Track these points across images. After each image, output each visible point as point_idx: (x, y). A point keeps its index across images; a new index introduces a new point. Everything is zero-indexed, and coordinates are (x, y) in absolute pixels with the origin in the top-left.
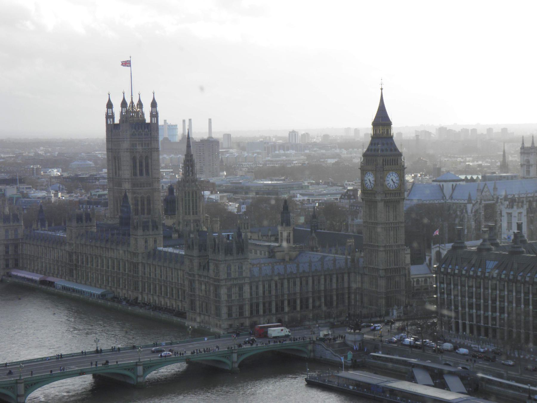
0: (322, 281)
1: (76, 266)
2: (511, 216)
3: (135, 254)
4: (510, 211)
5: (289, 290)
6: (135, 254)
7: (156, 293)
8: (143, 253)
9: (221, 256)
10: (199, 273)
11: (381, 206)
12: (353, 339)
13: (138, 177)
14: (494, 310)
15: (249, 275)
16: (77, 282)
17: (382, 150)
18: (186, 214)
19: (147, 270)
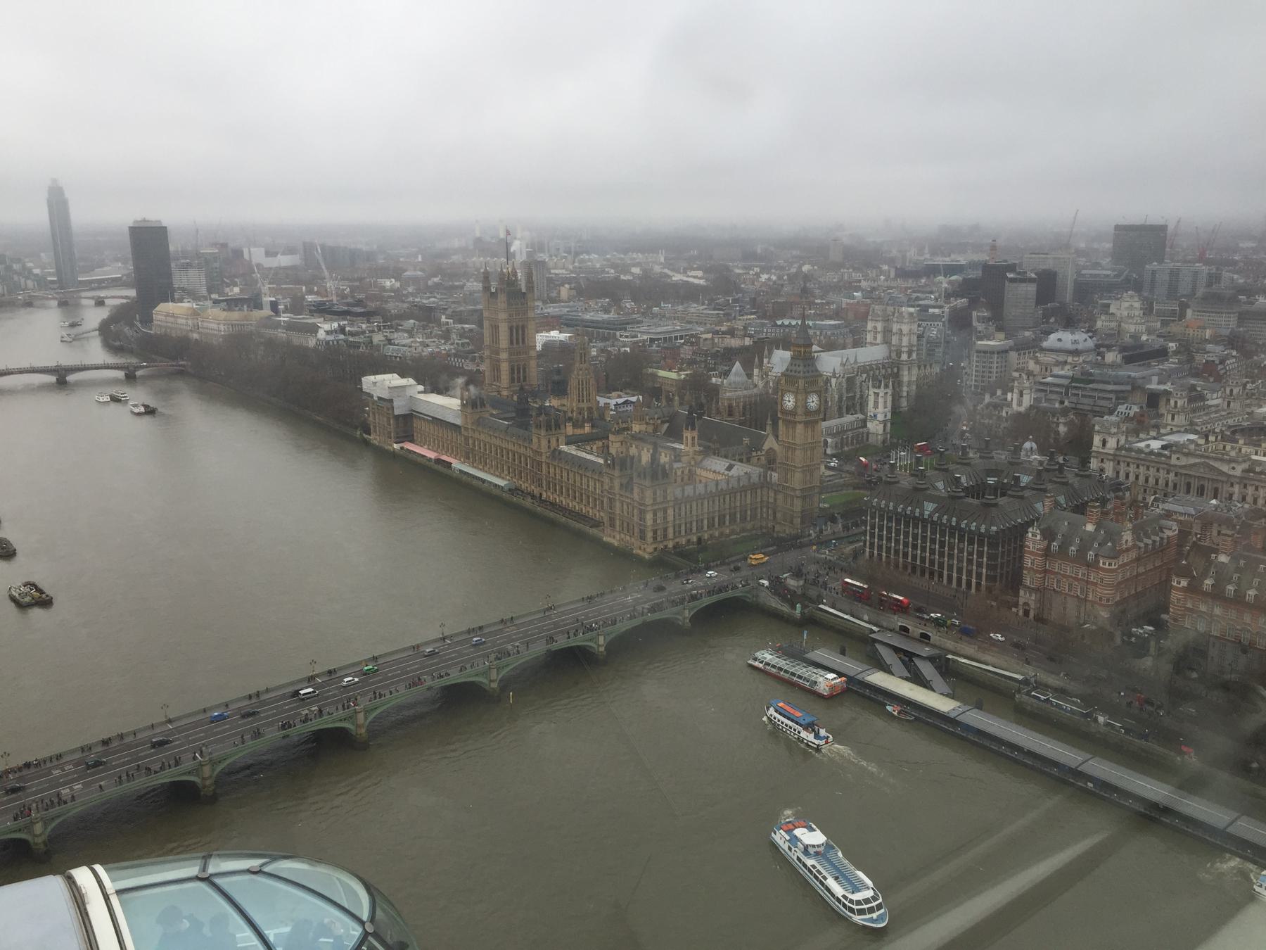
0: (738, 498)
1: (473, 450)
2: (878, 396)
3: (538, 452)
4: (876, 391)
5: (708, 509)
6: (540, 454)
7: (562, 493)
8: (546, 453)
9: (647, 483)
10: (621, 493)
11: (800, 428)
12: (796, 585)
13: (515, 346)
14: (932, 552)
15: (673, 499)
16: (473, 467)
17: (804, 372)
18: (579, 402)
19: (552, 470)
